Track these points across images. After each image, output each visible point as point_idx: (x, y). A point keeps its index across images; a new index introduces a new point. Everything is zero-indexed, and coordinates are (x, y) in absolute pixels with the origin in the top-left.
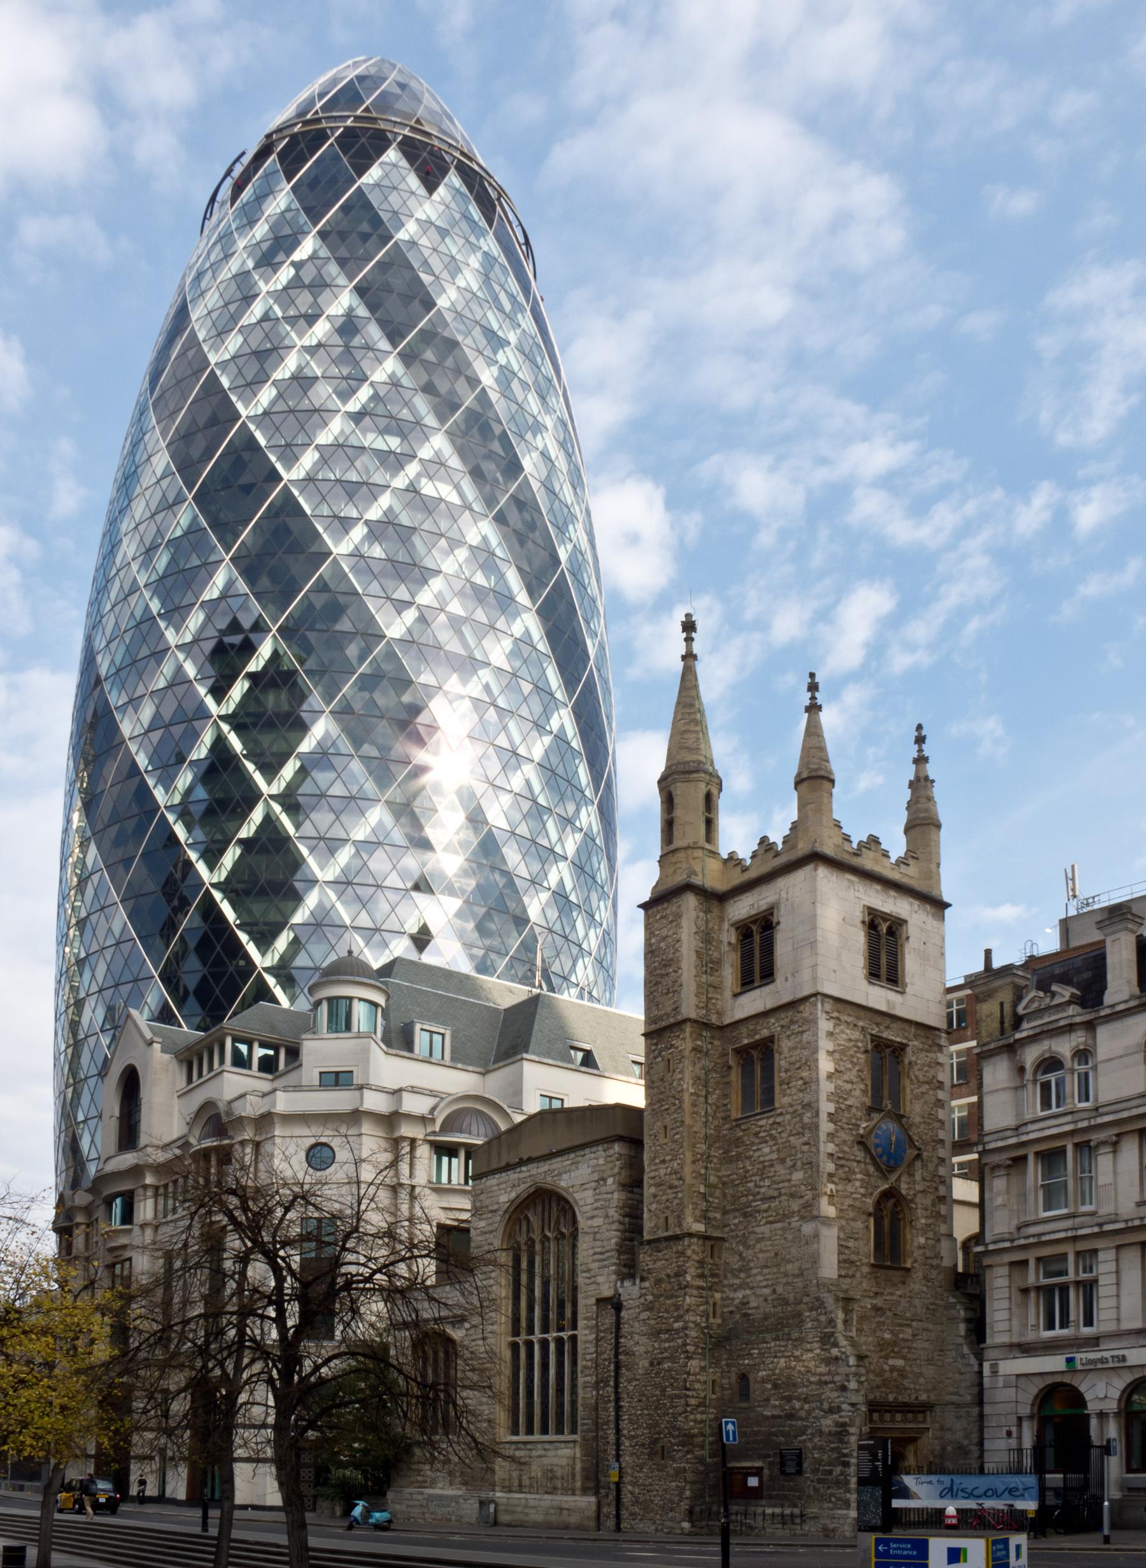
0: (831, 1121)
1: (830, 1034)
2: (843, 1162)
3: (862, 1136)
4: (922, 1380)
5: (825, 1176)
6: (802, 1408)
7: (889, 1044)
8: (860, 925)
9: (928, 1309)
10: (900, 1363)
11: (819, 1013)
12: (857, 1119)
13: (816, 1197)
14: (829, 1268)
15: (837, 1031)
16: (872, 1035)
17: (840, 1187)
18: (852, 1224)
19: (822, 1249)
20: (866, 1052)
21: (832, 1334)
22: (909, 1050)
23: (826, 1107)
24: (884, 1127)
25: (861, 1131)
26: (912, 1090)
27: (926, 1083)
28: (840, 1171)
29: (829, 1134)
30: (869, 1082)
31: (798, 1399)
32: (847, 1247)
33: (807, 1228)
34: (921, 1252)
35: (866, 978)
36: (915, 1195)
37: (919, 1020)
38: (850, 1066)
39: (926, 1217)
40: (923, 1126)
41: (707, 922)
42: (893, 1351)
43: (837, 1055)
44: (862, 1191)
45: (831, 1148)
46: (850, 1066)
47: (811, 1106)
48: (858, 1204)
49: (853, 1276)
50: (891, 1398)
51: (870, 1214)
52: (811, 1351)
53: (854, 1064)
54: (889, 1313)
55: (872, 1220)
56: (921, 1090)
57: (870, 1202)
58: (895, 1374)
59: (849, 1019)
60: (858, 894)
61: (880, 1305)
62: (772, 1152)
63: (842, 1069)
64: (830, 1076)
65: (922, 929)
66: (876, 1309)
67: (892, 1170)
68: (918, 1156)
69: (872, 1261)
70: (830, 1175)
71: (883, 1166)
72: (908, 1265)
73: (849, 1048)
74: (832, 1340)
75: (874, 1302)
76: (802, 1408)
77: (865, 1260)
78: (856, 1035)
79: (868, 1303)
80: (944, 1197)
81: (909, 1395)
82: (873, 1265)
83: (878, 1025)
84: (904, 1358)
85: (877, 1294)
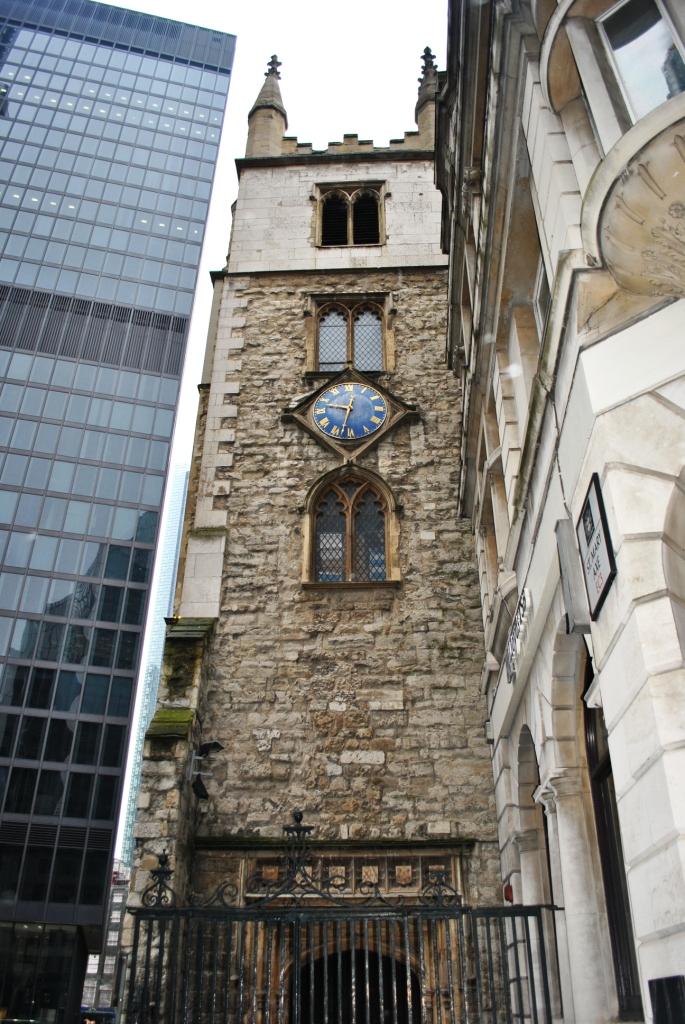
0: (232, 403)
4: (435, 790)
5: (211, 472)
9: (444, 648)
10: (376, 757)
18: (267, 530)
27: (430, 328)
32: (249, 566)
34: (427, 554)
42: (353, 735)
45: (227, 435)
46: (278, 336)
49: (257, 610)
50: (345, 833)
51: (301, 511)
54: (343, 665)
55: (307, 520)
58: (359, 783)
66: (314, 661)
70: (222, 469)
71: (332, 443)
72: (395, 575)
73: (276, 319)
75: (306, 648)
77: (289, 582)
78: (293, 301)
81: (401, 825)
82: (305, 587)
83: (332, 285)
84: (384, 747)
85: (314, 635)
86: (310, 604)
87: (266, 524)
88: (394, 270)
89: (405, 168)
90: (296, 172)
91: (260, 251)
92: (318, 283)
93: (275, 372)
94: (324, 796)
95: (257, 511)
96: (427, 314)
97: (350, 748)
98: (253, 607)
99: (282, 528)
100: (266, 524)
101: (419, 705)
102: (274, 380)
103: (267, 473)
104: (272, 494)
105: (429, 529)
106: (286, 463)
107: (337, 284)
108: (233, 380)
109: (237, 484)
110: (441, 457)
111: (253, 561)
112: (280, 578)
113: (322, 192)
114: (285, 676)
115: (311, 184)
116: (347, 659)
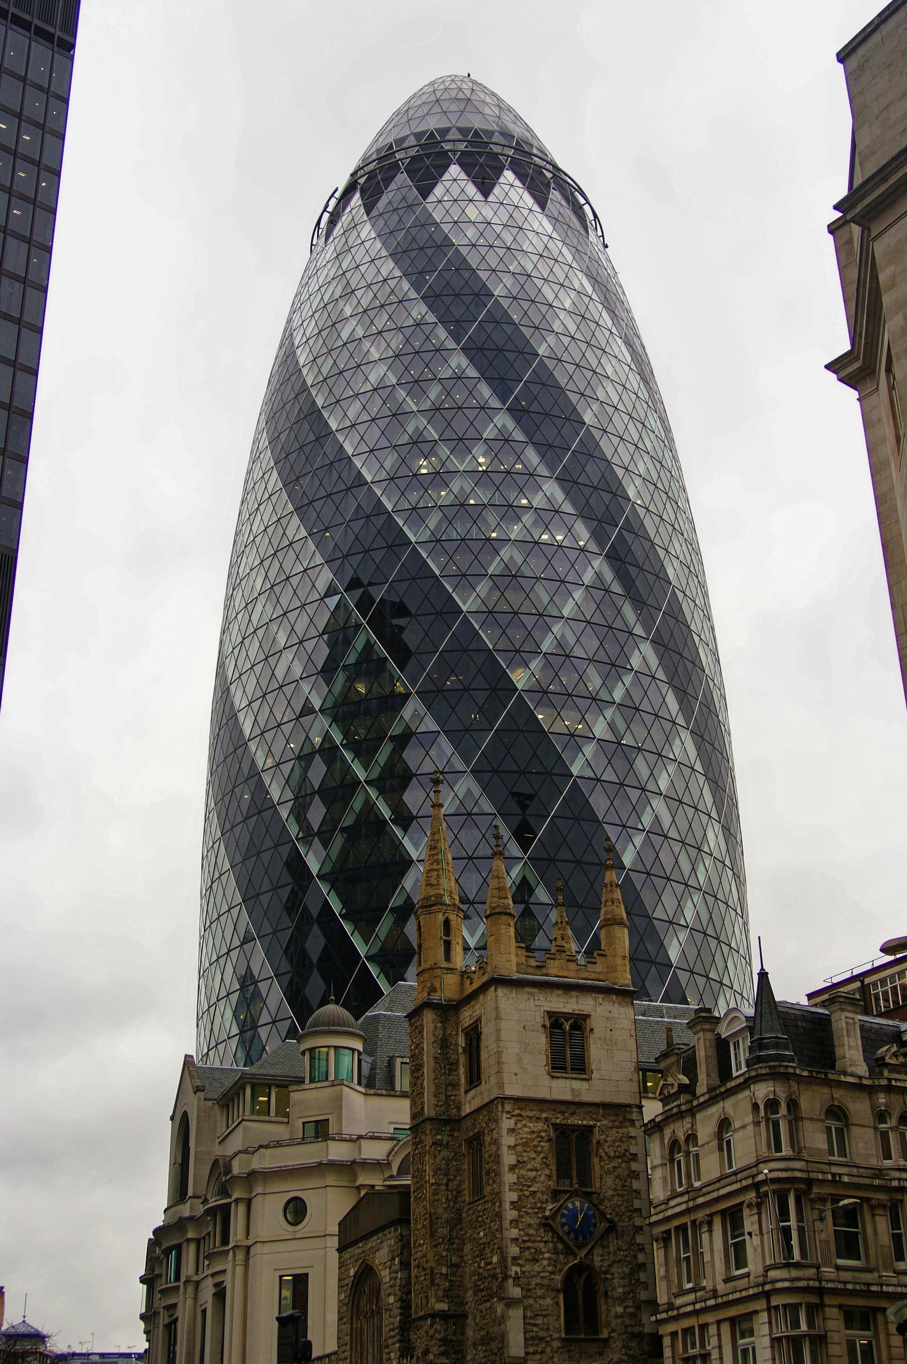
0: (514, 1208)
1: (511, 1131)
2: (529, 1244)
3: (546, 1218)
7: (575, 1128)
8: (541, 1029)
12: (542, 1203)
13: (506, 1277)
15: (519, 1126)
16: (553, 1124)
17: (527, 1268)
20: (550, 1140)
24: (570, 1206)
25: (547, 1213)
26: (602, 1167)
27: (618, 1157)
28: (526, 1253)
30: (553, 1167)
32: (535, 1325)
35: (548, 1073)
36: (610, 1266)
37: (607, 1099)
38: (534, 1155)
39: (624, 1286)
40: (616, 1198)
41: (445, 1029)
43: (520, 1148)
44: (550, 1268)
45: (514, 1233)
46: (534, 1155)
48: (546, 1282)
49: (543, 1352)
51: (558, 1291)
53: (540, 1153)
55: (561, 1296)
56: (613, 1165)
57: (558, 1277)
59: (531, 1114)
60: (537, 1003)
62: (485, 1235)
63: (525, 1159)
64: (512, 1168)
65: (607, 1018)
67: (580, 1247)
69: (563, 1336)
72: (605, 1335)
73: (532, 1140)
77: (556, 1335)
78: (540, 1126)
80: (644, 1264)
82: (564, 1340)
83: (562, 1113)
86: (565, 1349)
87: (540, 1297)
89: (601, 1001)
90: (532, 994)
91: (516, 1074)
92: (554, 1110)
93: (536, 1185)
95: (535, 1289)
96: (616, 1144)
98: (540, 1350)
99: (548, 1300)
100: (540, 1297)
102: (535, 1192)
103: (537, 1261)
104: (542, 1277)
105: (620, 1305)
106: (547, 1255)
107: (565, 1112)
108: (514, 1190)
109: (524, 1269)
110: (626, 1256)
111: (538, 1322)
112: (551, 1333)
113: (550, 1018)
115: (542, 1009)
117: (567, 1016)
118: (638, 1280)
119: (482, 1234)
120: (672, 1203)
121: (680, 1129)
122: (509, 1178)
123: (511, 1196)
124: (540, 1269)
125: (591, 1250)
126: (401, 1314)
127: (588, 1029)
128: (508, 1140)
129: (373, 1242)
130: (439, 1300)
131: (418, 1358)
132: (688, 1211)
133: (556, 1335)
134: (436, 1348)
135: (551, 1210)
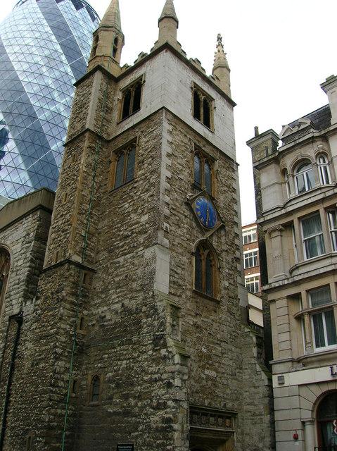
2: (176, 213)
6: (136, 405)
10: (213, 374)
11: (164, 117)
14: (162, 284)
17: (173, 228)
19: (157, 268)
20: (192, 152)
21: (162, 337)
22: (217, 163)
23: (165, 173)
29: (166, 189)
31: (135, 398)
32: (176, 273)
33: (148, 253)
45: (167, 199)
47: (155, 171)
51: (192, 254)
52: (143, 353)
55: (194, 259)
57: (193, 246)
58: (210, 382)
61: (199, 323)
64: (169, 155)
68: (223, 227)
74: (162, 342)
76: (136, 405)
77: (189, 287)
78: (186, 140)
79: (191, 320)
84: (216, 370)
85: (197, 314)
88: (221, 152)
94: (201, 387)
97: (208, 368)
101: (224, 355)
106: (186, 226)
114: (189, 331)
116: (206, 329)
117: (204, 93)
118: (236, 268)
119: (127, 205)
120: (293, 203)
121: (310, 152)
122: (165, 161)
123: (165, 173)
124: (181, 234)
125: (212, 235)
126: (29, 271)
127: (213, 106)
128: (166, 137)
129: (8, 232)
130: (76, 253)
131: (46, 298)
132: (323, 200)
133: (189, 287)
134: (68, 288)
135: (190, 196)
